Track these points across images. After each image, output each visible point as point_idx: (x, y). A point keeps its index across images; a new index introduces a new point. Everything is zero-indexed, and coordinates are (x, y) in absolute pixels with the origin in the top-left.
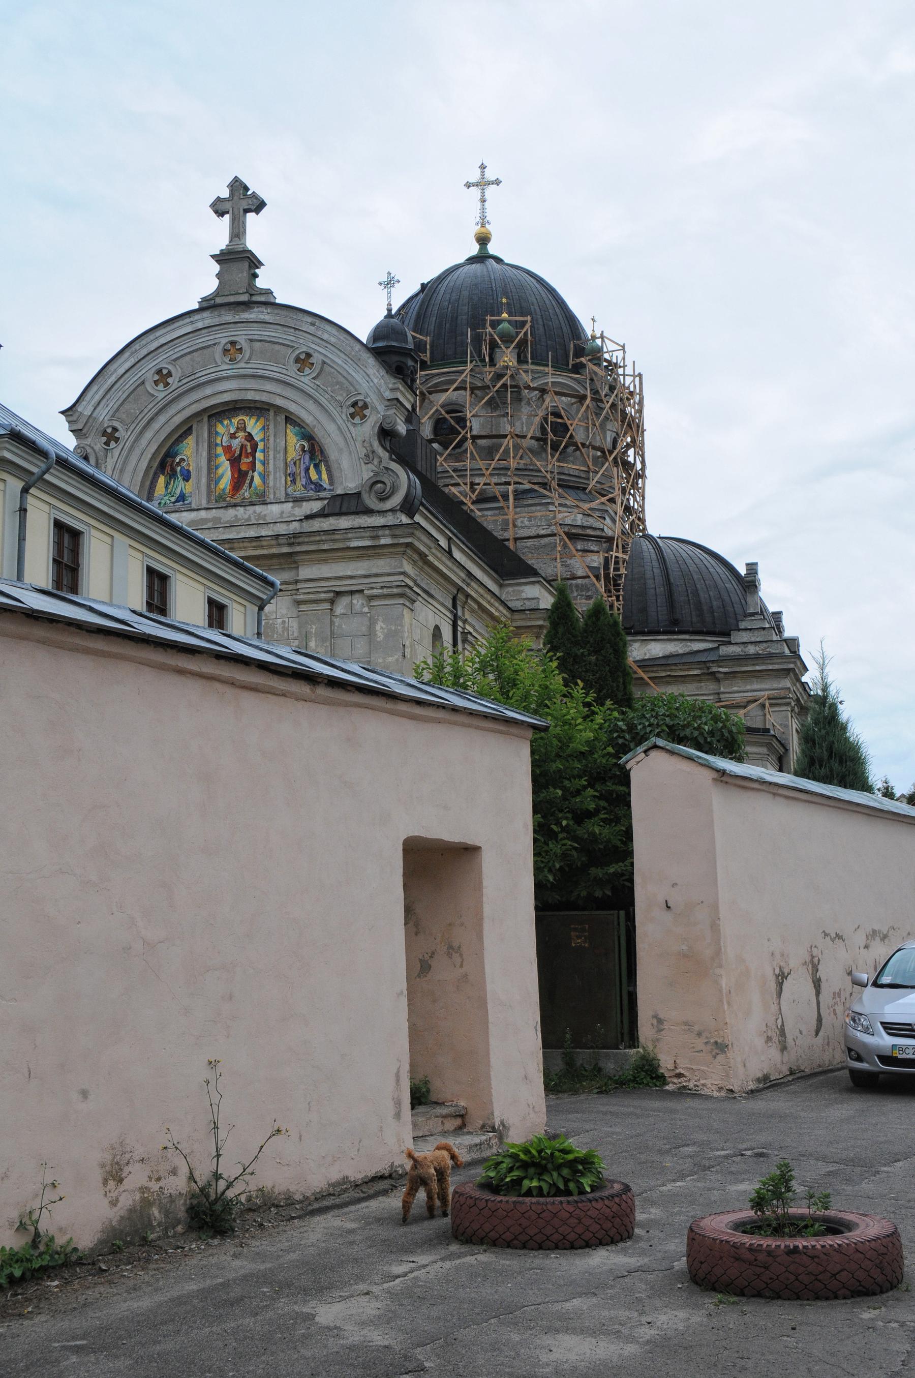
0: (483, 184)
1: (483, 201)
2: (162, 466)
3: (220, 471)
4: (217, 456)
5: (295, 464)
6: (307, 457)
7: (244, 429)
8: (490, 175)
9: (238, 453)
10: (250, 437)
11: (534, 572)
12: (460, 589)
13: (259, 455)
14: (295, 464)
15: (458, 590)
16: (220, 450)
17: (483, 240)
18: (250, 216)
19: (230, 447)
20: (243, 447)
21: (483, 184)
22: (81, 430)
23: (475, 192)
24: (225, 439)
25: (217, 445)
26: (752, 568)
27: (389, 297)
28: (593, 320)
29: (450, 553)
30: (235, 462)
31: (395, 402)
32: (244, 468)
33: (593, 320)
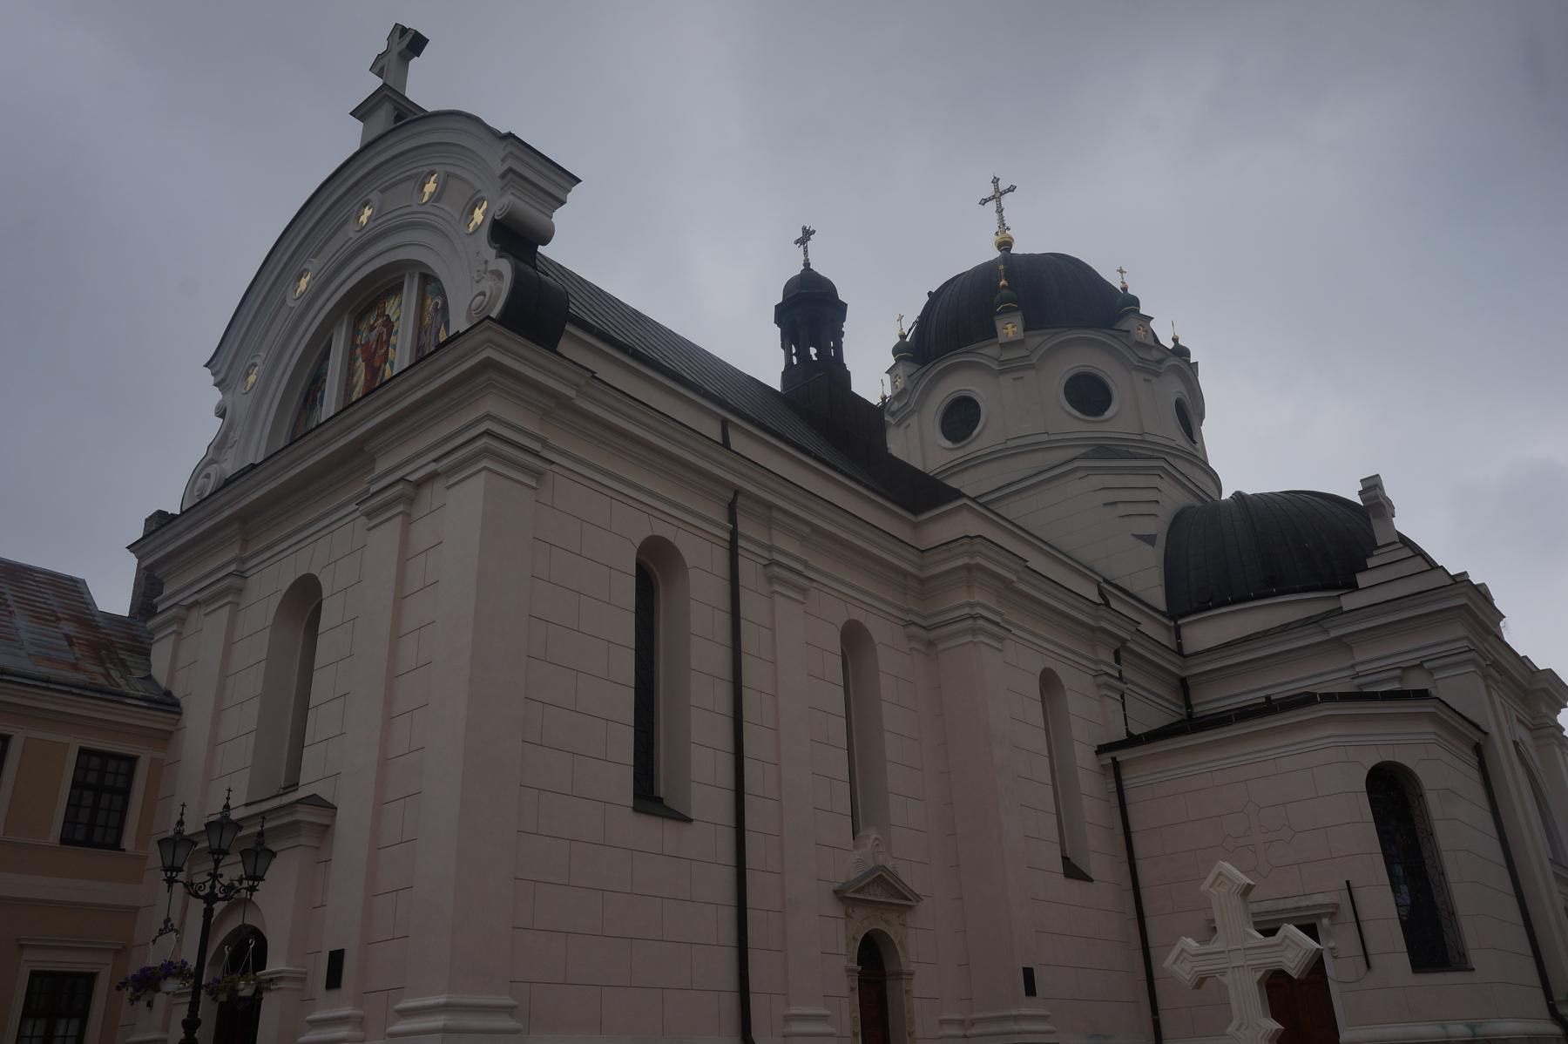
0: (998, 195)
1: (1000, 211)
8: (1003, 186)
11: (958, 494)
12: (737, 492)
15: (736, 493)
16: (358, 351)
17: (1004, 245)
18: (414, 63)
20: (380, 334)
21: (998, 195)
23: (992, 205)
26: (1372, 486)
27: (806, 252)
28: (1121, 271)
29: (726, 444)
30: (369, 362)
31: (510, 176)
33: (1121, 271)
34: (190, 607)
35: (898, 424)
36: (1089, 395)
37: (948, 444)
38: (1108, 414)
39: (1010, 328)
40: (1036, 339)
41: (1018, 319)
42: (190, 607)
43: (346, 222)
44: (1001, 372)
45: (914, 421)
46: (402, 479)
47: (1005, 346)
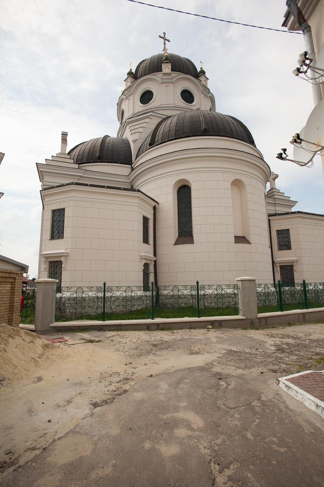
35: (126, 99)
36: (187, 96)
37: (142, 105)
38: (193, 104)
39: (167, 68)
40: (174, 74)
41: (169, 66)
44: (162, 83)
45: (131, 97)
47: (164, 74)
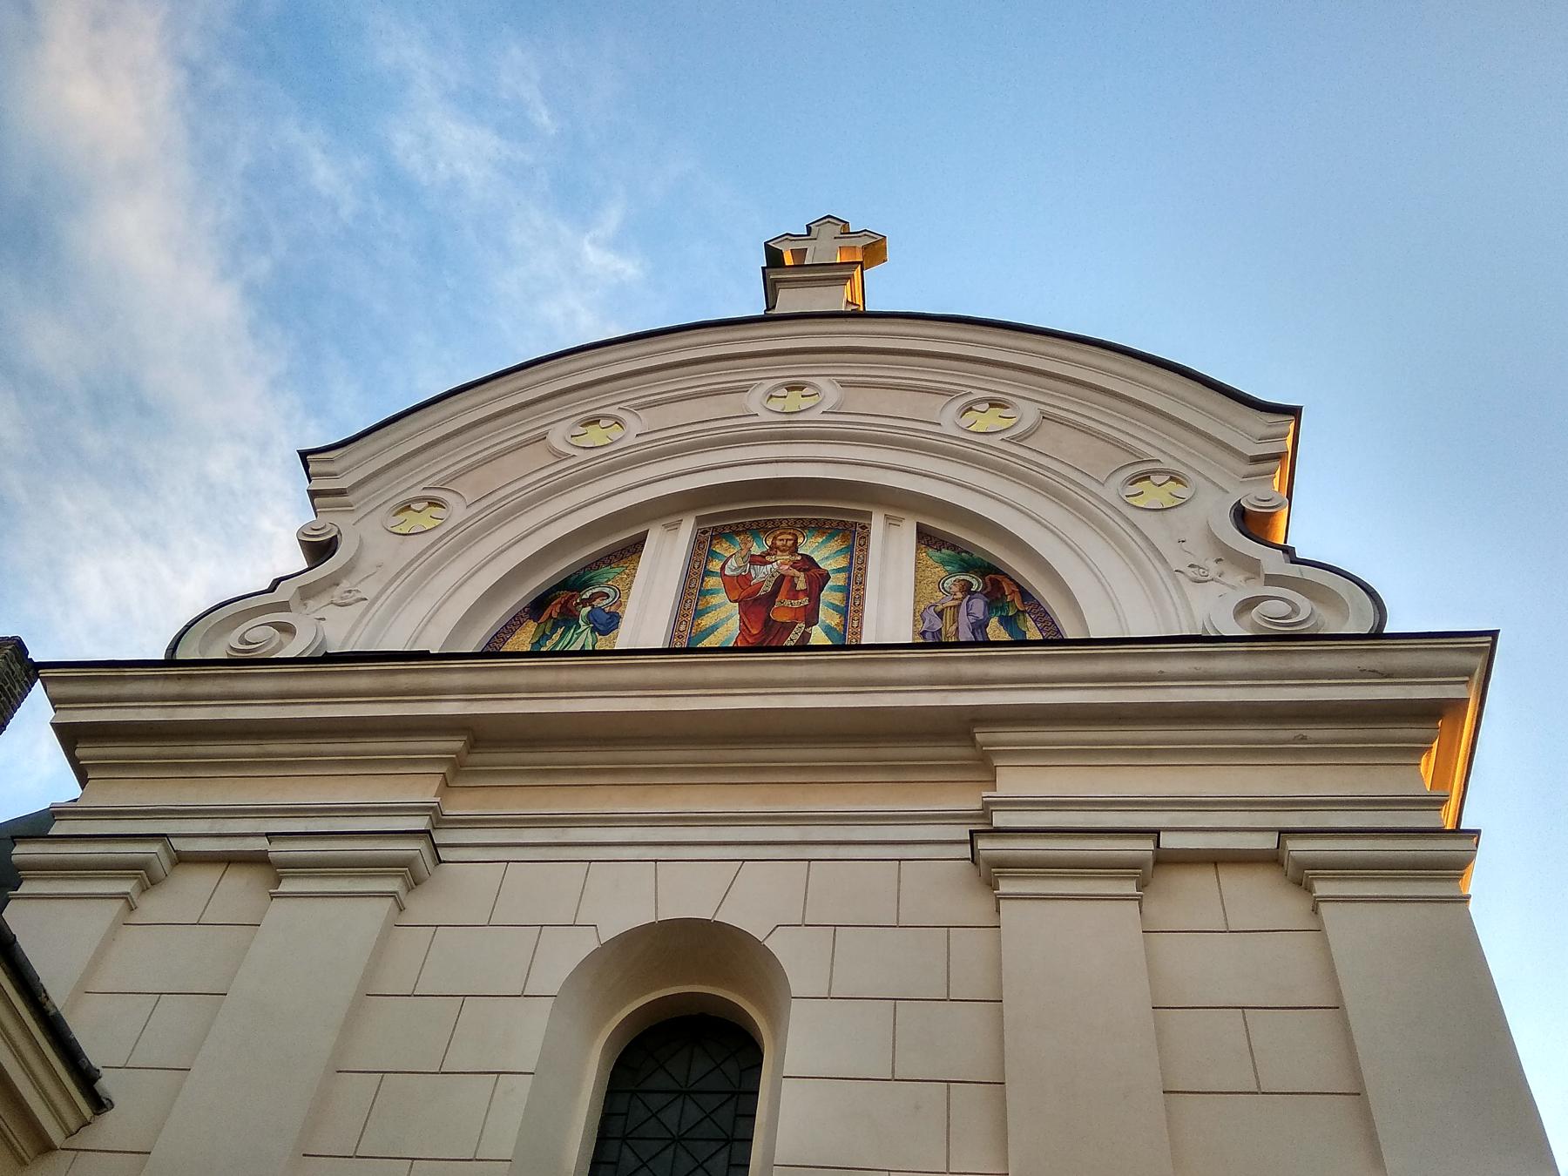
2: (537, 607)
3: (706, 621)
4: (703, 593)
5: (940, 614)
6: (979, 606)
7: (794, 549)
9: (767, 588)
10: (808, 563)
13: (828, 596)
14: (940, 614)
19: (744, 580)
22: (341, 493)
24: (732, 563)
25: (708, 573)
32: (779, 615)
34: (182, 859)
42: (182, 859)
43: (744, 390)
46: (1155, 833)
